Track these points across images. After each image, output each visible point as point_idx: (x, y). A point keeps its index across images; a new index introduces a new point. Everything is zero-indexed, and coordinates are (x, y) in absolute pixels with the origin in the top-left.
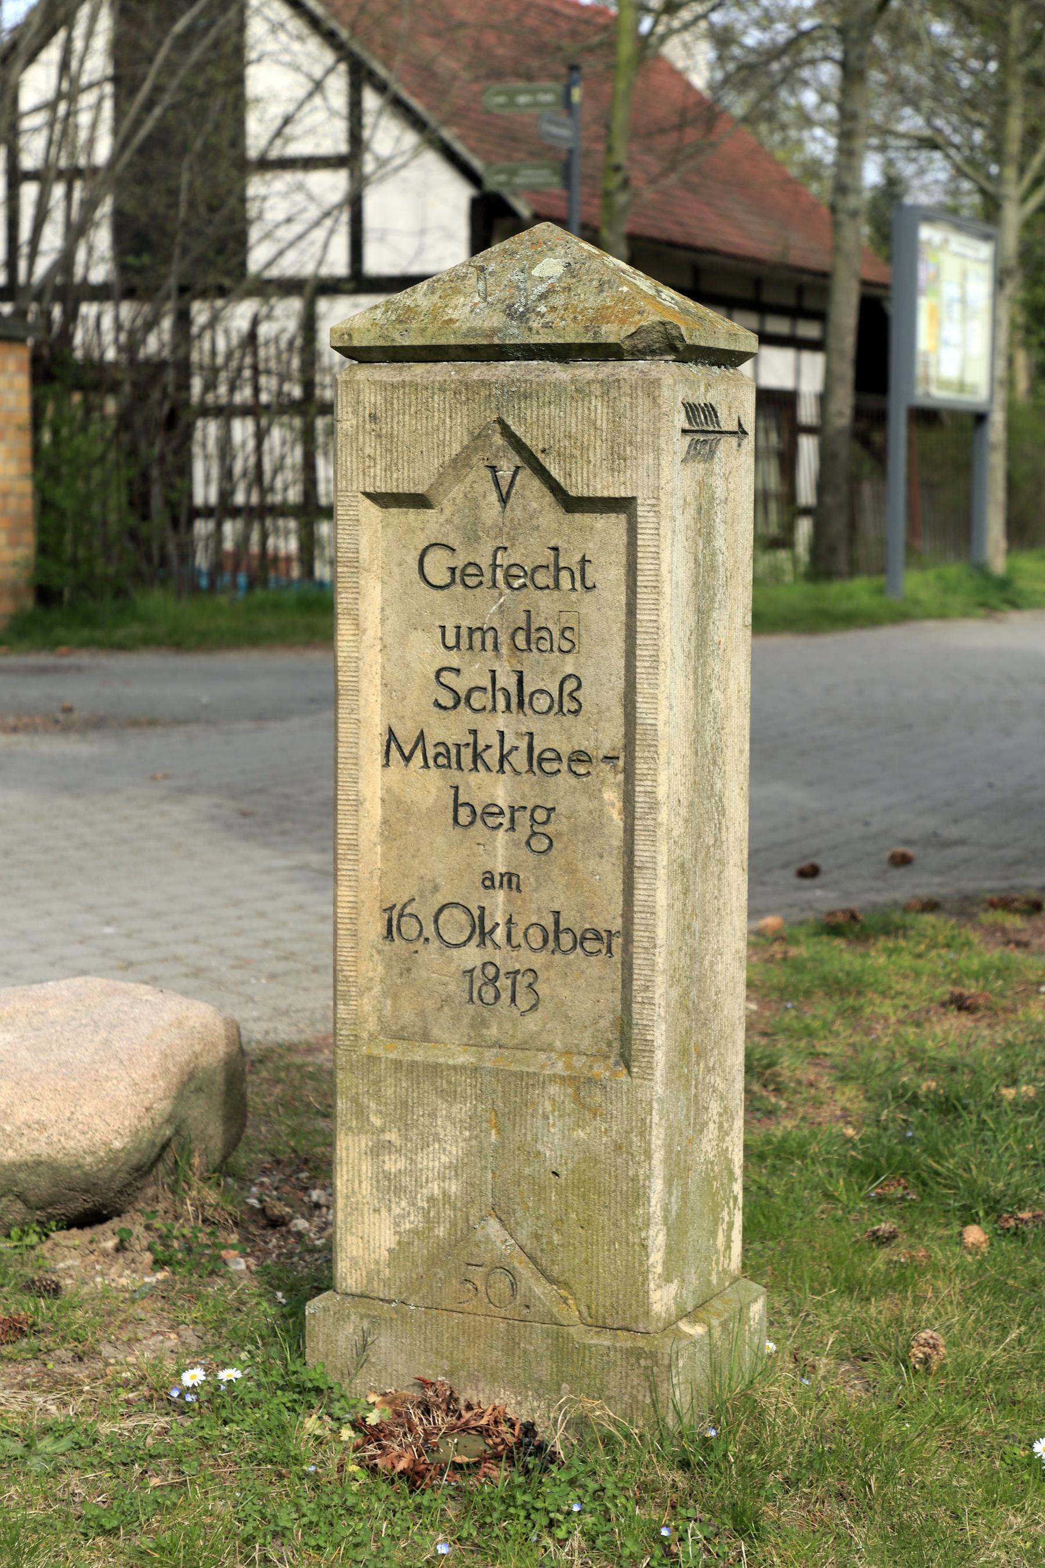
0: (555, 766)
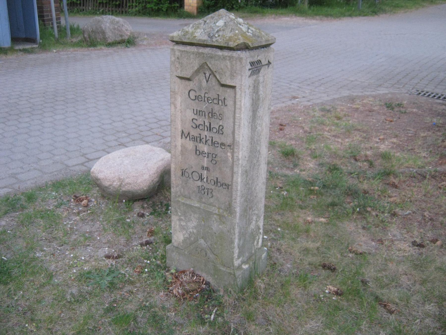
0: (217, 145)
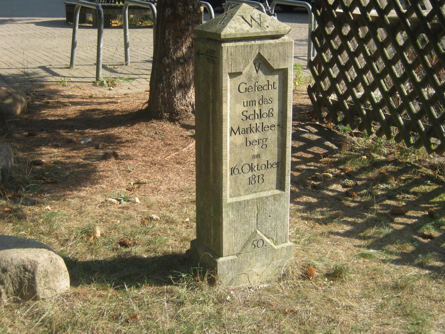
0: (268, 129)
